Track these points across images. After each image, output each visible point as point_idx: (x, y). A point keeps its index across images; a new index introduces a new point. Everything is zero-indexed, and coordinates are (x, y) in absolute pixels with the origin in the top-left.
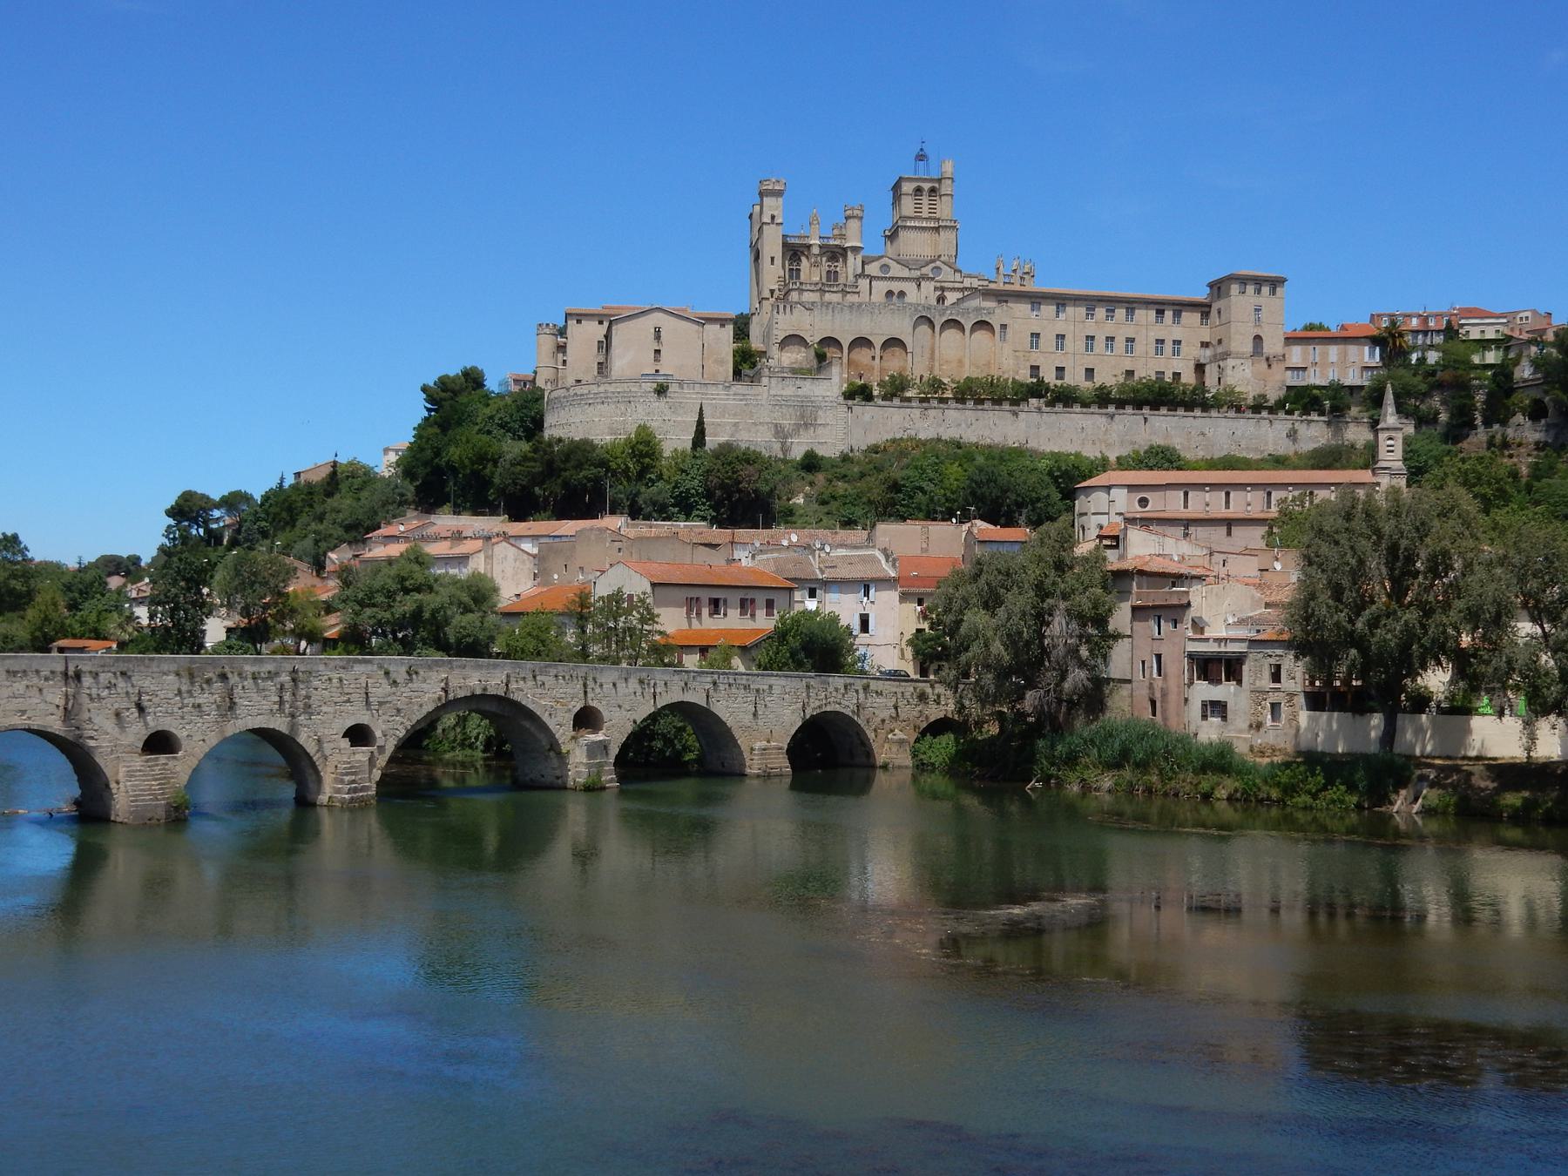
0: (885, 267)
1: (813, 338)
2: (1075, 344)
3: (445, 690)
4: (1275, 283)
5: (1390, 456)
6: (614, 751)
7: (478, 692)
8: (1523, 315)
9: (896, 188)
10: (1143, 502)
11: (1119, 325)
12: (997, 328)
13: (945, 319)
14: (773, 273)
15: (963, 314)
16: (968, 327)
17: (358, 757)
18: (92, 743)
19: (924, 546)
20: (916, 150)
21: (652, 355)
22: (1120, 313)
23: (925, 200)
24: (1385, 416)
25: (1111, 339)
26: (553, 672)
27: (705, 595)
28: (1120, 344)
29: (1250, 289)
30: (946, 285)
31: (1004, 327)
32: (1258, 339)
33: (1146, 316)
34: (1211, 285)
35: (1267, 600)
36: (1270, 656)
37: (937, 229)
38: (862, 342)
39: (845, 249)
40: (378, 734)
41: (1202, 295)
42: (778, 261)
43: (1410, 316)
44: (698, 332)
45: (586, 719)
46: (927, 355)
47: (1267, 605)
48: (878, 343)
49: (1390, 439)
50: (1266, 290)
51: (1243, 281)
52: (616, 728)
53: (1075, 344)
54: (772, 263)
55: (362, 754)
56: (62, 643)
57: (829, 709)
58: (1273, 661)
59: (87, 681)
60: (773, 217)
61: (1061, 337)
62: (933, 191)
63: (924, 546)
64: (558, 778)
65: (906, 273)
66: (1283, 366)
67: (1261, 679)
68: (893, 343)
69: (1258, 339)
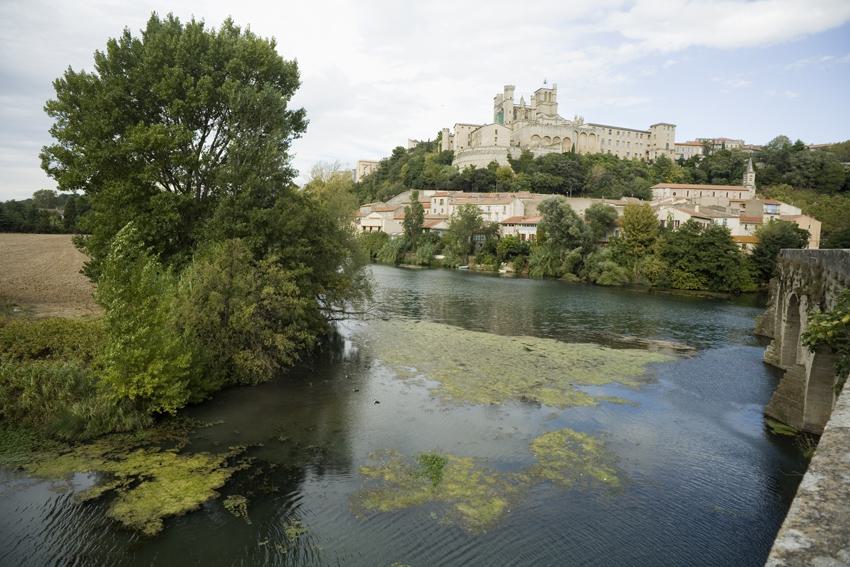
10: (675, 194)
32: (668, 145)
48: (562, 138)
53: (613, 143)
69: (668, 145)
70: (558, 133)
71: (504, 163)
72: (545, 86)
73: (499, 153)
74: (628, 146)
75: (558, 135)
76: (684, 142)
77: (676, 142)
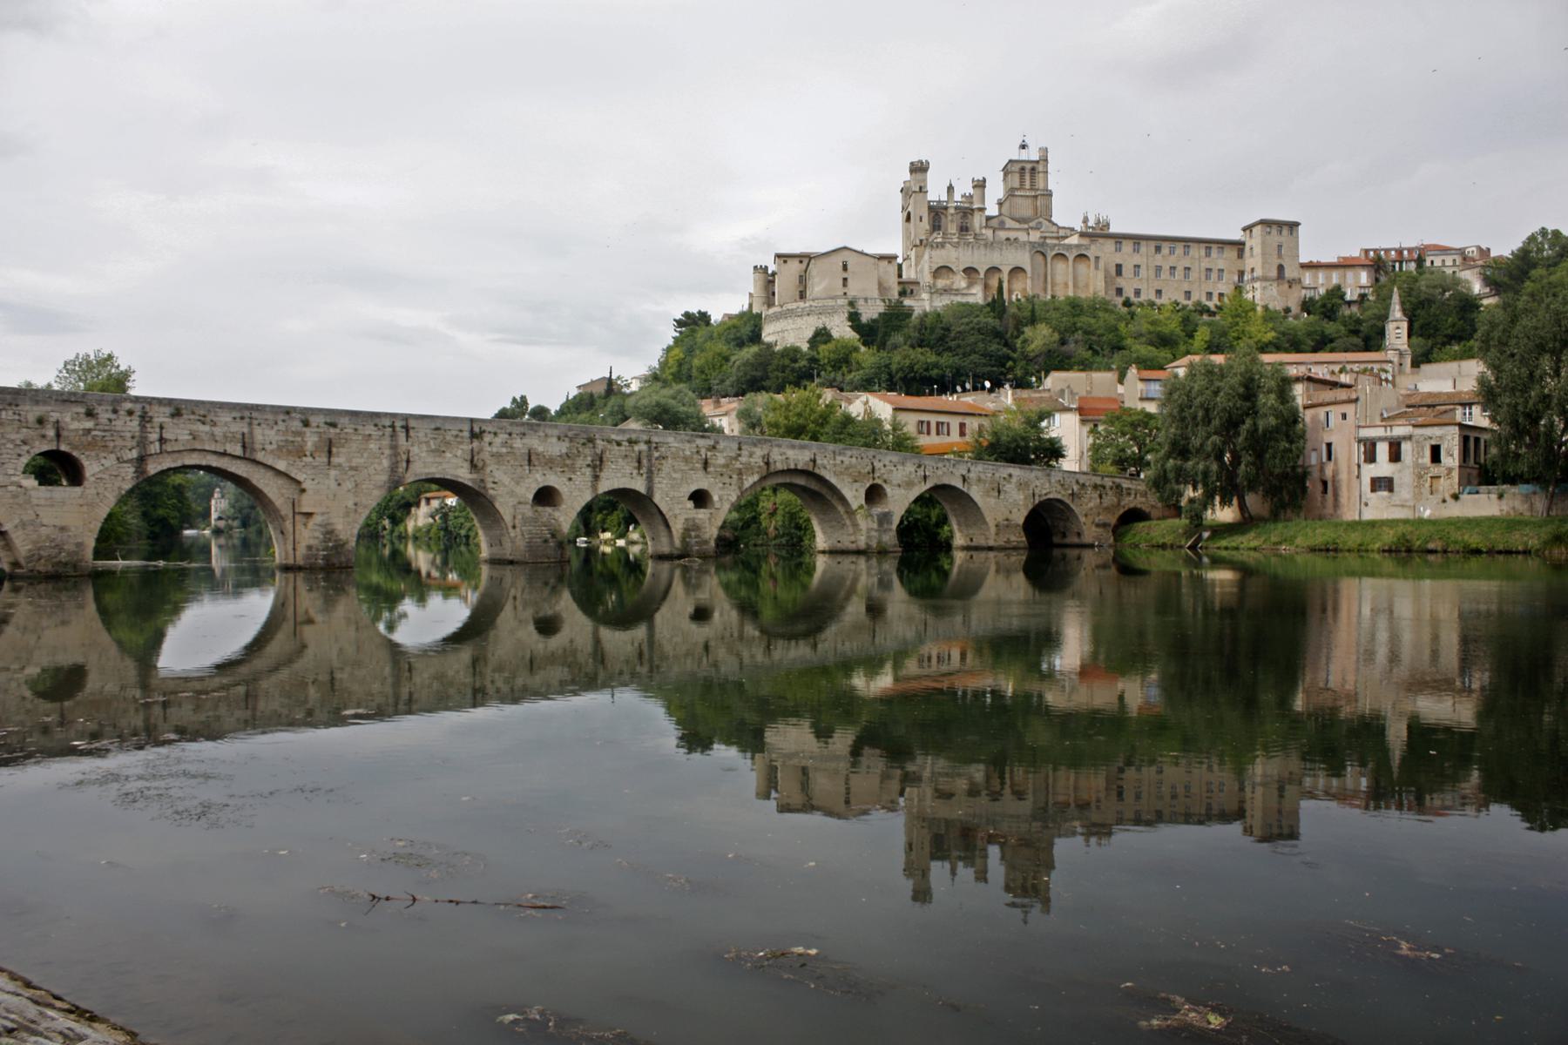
0: (1002, 223)
1: (958, 267)
3: (767, 464)
4: (1293, 226)
5: (1398, 341)
6: (896, 521)
7: (792, 467)
8: (1470, 250)
11: (1178, 259)
12: (1092, 259)
13: (1054, 253)
15: (1067, 250)
16: (1071, 258)
17: (700, 516)
18: (491, 492)
19: (1088, 389)
20: (1020, 142)
21: (841, 282)
22: (1180, 248)
23: (1027, 177)
24: (1394, 311)
25: (1173, 268)
26: (849, 453)
27: (933, 419)
28: (1179, 273)
29: (1274, 230)
30: (1047, 235)
31: (1097, 258)
32: (1281, 268)
33: (1197, 252)
34: (1244, 229)
35: (1409, 403)
36: (1431, 438)
37: (1036, 197)
38: (994, 270)
39: (973, 210)
40: (716, 498)
41: (1237, 235)
42: (925, 219)
43: (1387, 251)
44: (874, 264)
45: (874, 494)
46: (1042, 279)
47: (1408, 406)
48: (1006, 270)
49: (1398, 328)
50: (1285, 231)
52: (898, 502)
54: (921, 220)
55: (702, 514)
56: (428, 495)
57: (1051, 496)
58: (1433, 443)
59: (487, 438)
60: (921, 188)
61: (1137, 266)
62: (1033, 169)
63: (1088, 389)
64: (853, 542)
65: (1017, 225)
66: (1299, 287)
67: (1423, 457)
68: (1017, 271)
69: (1281, 268)
70: (995, 258)
71: (841, 330)
72: (1024, 155)
73: (832, 311)
74: (1186, 276)
75: (996, 263)
76: (1334, 260)
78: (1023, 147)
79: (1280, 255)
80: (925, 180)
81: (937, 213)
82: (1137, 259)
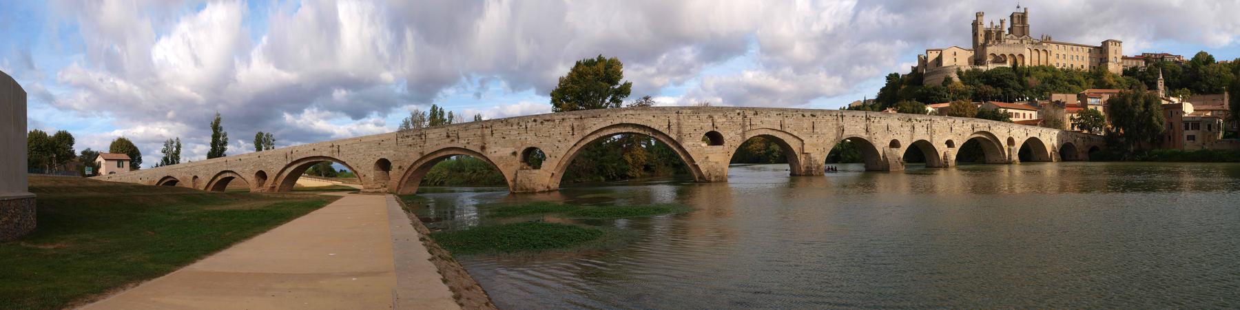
2: (1068, 57)
3: (973, 129)
9: (1012, 17)
14: (981, 40)
28: (1080, 58)
42: (979, 35)
51: (1112, 41)
53: (1068, 57)
76: (1133, 56)
77: (1125, 54)
78: (1018, 7)
79: (1116, 53)
80: (982, 20)
81: (988, 33)
82: (1064, 53)
